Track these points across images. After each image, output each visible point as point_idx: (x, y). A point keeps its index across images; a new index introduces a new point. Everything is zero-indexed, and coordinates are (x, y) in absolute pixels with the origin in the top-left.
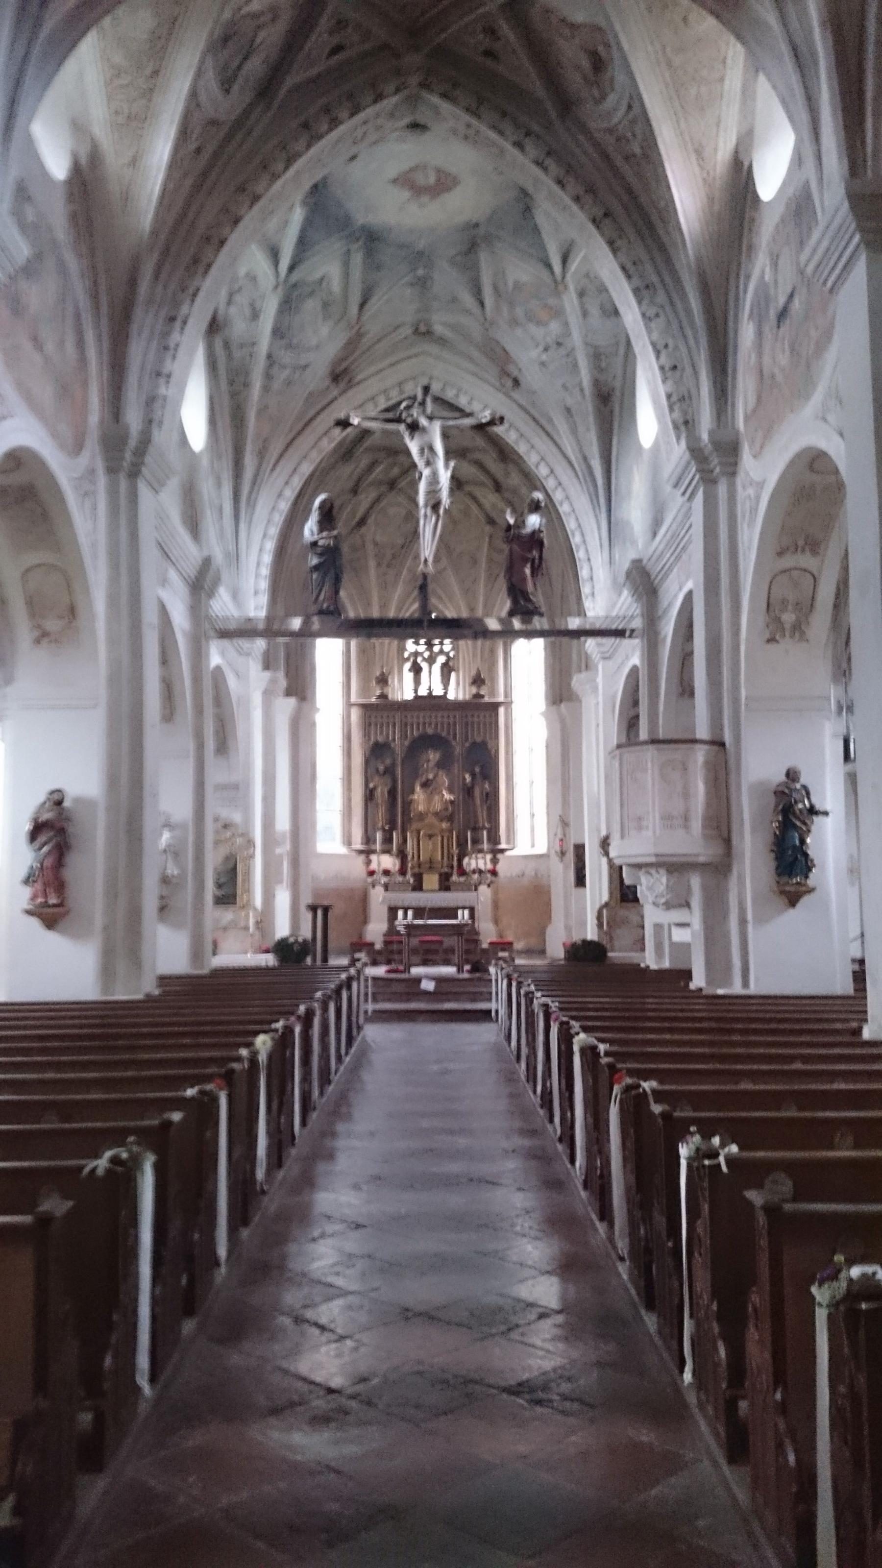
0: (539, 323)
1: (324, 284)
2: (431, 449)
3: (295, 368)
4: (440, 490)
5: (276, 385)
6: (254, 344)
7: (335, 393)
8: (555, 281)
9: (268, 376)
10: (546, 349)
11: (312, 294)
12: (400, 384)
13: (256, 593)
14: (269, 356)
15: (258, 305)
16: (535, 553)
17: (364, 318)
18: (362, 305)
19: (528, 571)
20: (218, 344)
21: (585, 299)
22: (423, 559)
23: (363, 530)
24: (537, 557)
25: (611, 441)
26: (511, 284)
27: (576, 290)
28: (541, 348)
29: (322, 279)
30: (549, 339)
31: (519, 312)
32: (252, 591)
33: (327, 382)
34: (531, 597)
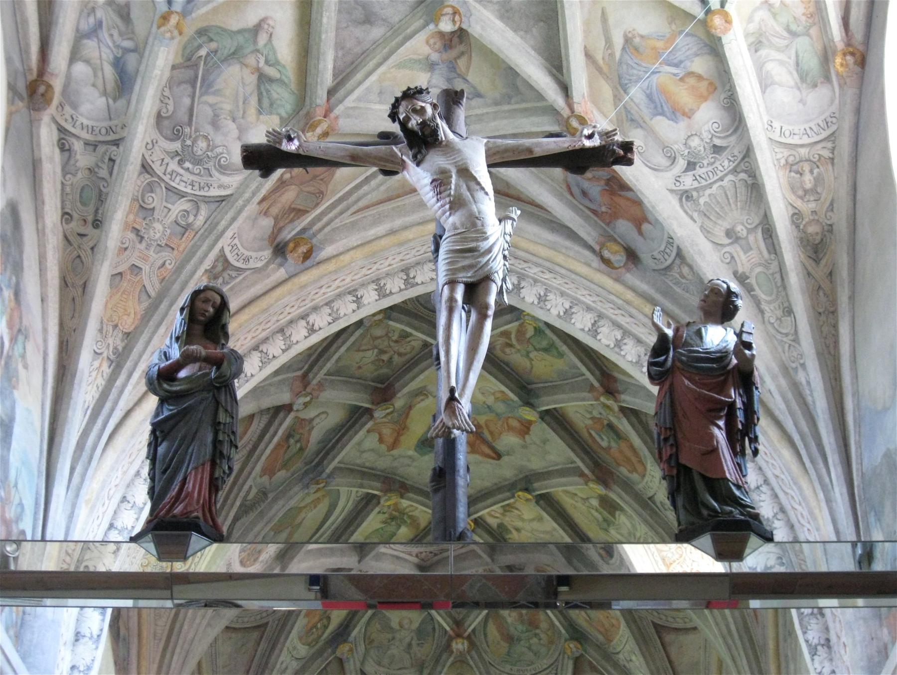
0: (677, 113)
1: (262, 39)
2: (465, 173)
3: (196, 202)
4: (489, 250)
5: (158, 230)
6: (116, 143)
7: (281, 273)
8: (708, 12)
9: (144, 210)
10: (691, 166)
11: (235, 55)
12: (406, 270)
13: (78, 636)
14: (146, 168)
15: (131, 60)
16: (735, 396)
17: (339, 110)
18: (331, 92)
19: (720, 435)
20: (47, 135)
21: (763, 52)
22: (444, 396)
23: (343, 650)
24: (739, 404)
25: (835, 326)
26: (618, 41)
27: (747, 35)
28: (682, 163)
29: (257, 29)
30: (695, 142)
31: (636, 92)
32: (69, 635)
33: (267, 253)
34: (737, 493)
